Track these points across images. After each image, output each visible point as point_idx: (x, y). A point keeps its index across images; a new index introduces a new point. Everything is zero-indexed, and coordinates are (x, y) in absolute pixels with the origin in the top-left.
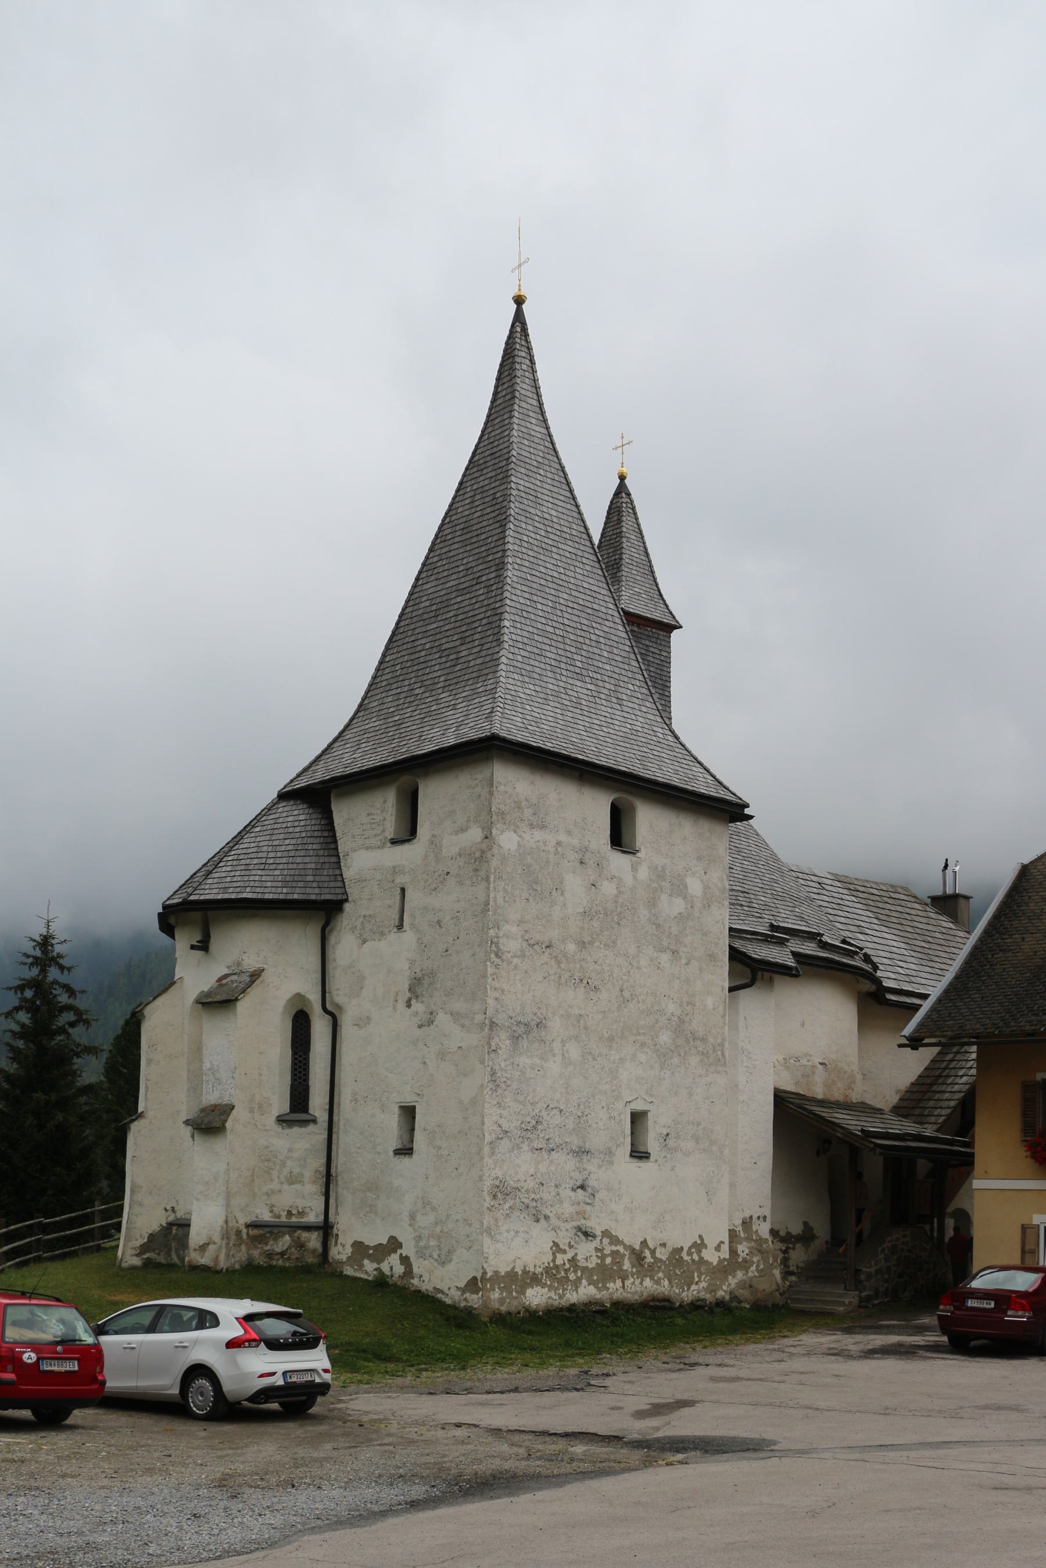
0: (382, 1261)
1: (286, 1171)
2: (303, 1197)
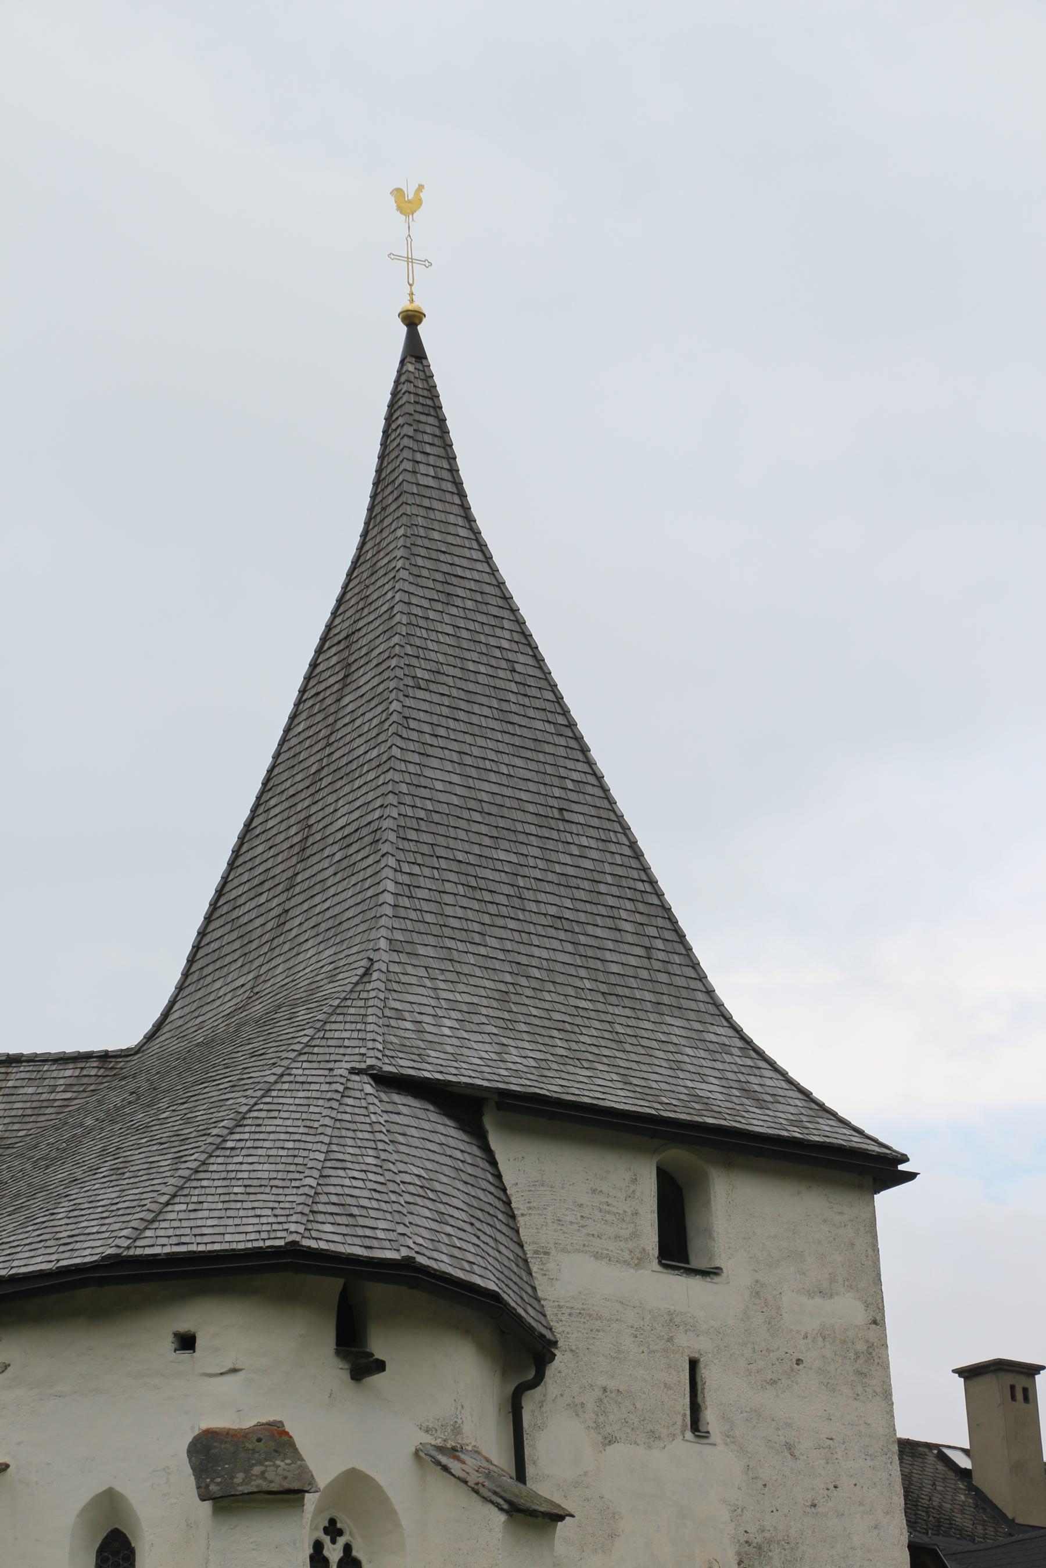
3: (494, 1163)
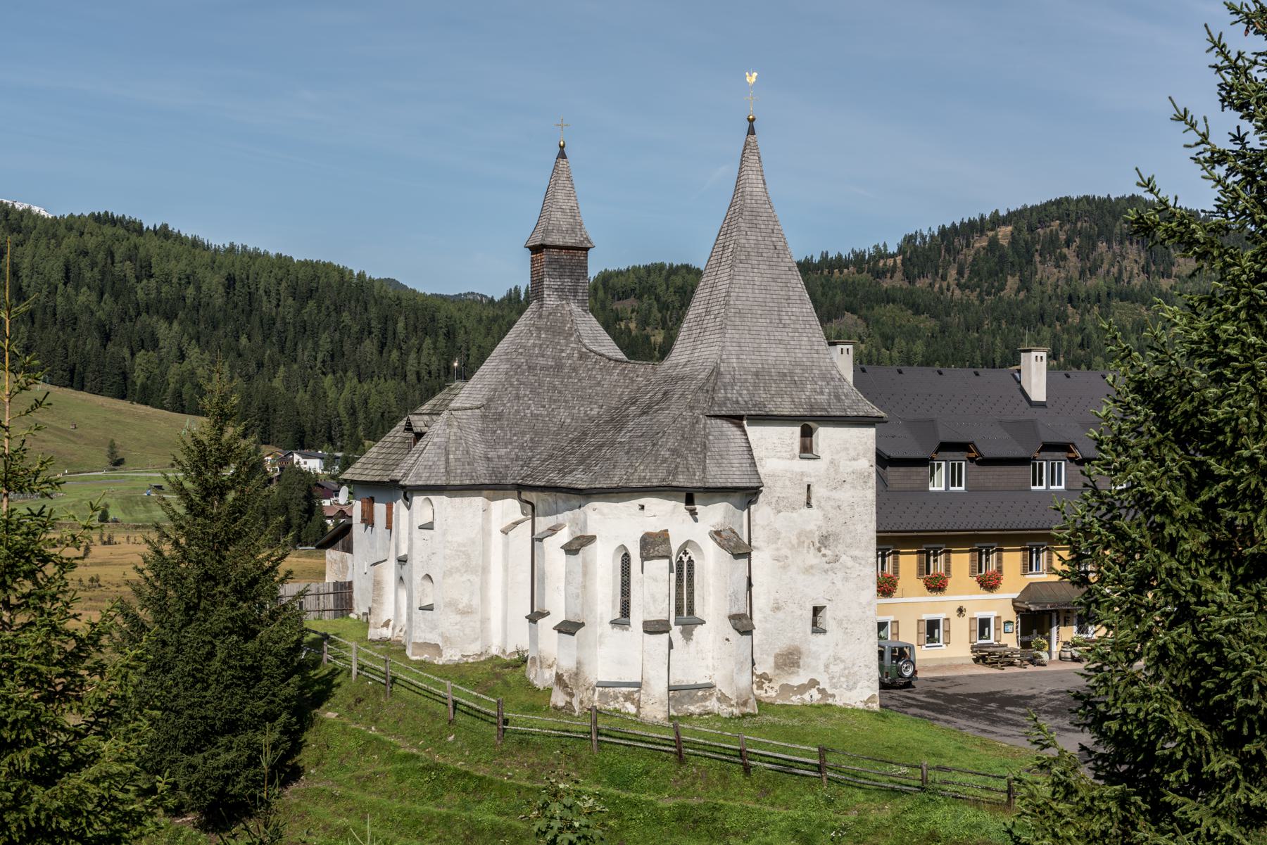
3: (746, 435)
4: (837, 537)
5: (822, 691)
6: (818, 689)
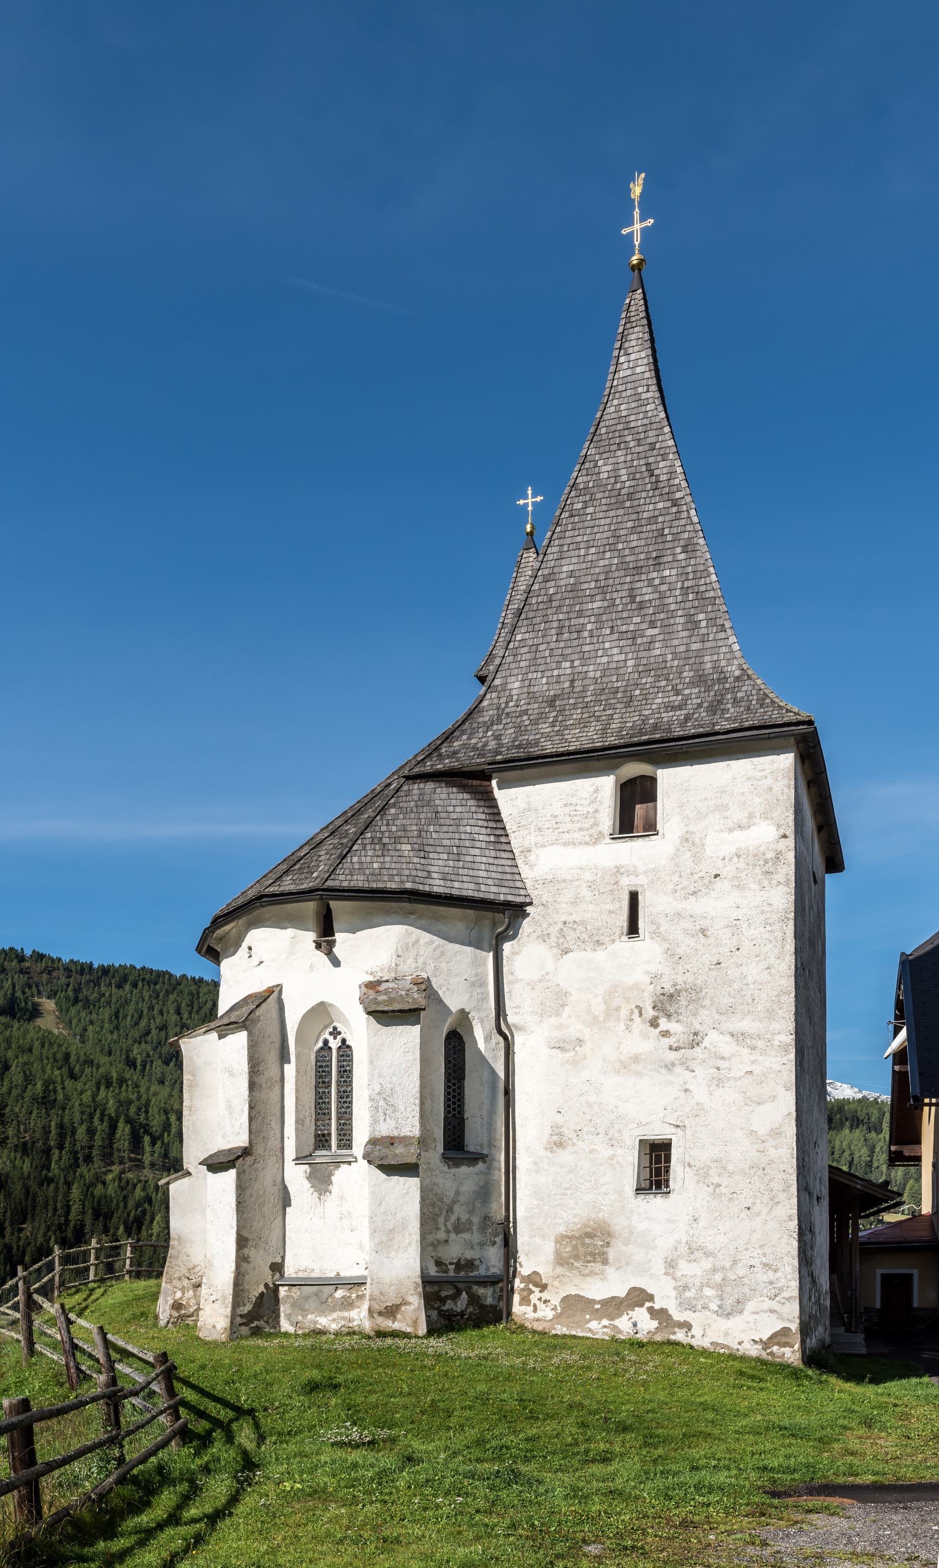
0: (620, 1315)
1: (453, 1218)
2: (472, 1247)
4: (695, 994)
5: (660, 1315)
6: (651, 1310)
